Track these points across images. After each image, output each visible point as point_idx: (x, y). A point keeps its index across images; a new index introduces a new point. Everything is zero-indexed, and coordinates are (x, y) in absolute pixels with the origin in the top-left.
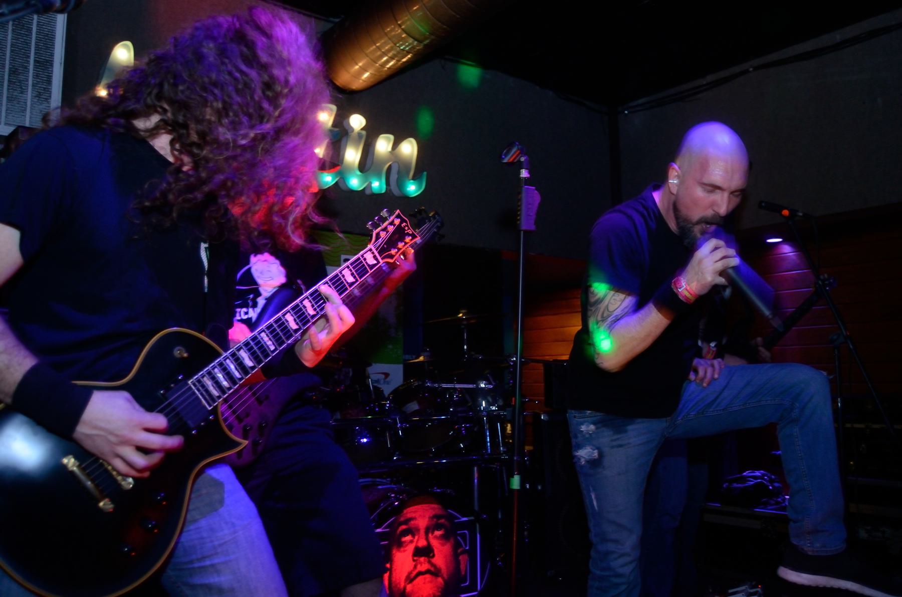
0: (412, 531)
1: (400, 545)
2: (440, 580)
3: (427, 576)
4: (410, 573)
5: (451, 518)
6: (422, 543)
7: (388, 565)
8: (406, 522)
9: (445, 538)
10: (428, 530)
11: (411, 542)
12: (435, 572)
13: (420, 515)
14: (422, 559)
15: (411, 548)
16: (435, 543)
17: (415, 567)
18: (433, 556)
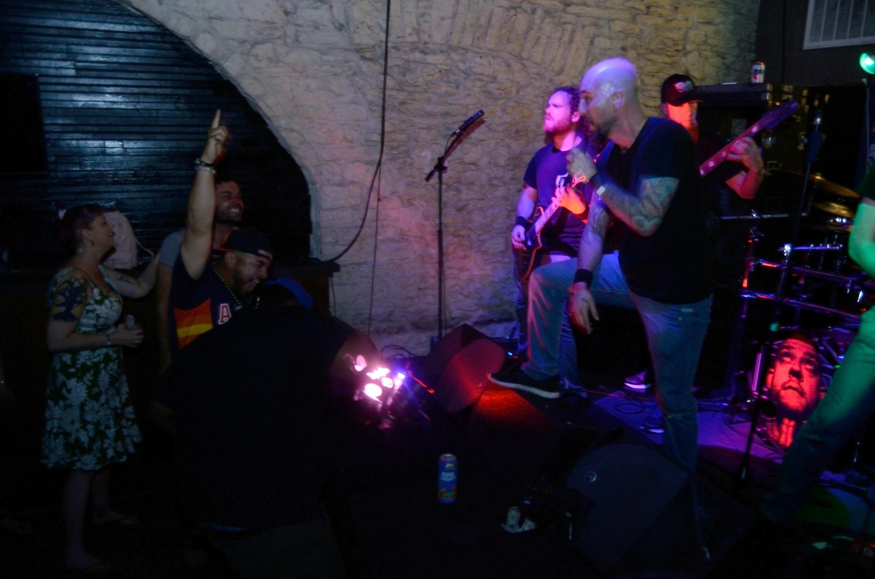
0: (792, 357)
1: (782, 362)
2: (803, 401)
3: (796, 394)
4: (785, 383)
5: (820, 361)
6: (796, 368)
7: (772, 370)
8: (789, 348)
9: (814, 372)
10: (803, 361)
11: (789, 363)
12: (802, 393)
13: (799, 348)
14: (794, 379)
15: (788, 367)
16: (805, 373)
17: (790, 381)
18: (802, 381)
